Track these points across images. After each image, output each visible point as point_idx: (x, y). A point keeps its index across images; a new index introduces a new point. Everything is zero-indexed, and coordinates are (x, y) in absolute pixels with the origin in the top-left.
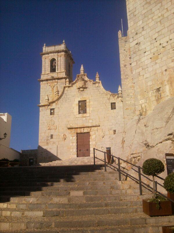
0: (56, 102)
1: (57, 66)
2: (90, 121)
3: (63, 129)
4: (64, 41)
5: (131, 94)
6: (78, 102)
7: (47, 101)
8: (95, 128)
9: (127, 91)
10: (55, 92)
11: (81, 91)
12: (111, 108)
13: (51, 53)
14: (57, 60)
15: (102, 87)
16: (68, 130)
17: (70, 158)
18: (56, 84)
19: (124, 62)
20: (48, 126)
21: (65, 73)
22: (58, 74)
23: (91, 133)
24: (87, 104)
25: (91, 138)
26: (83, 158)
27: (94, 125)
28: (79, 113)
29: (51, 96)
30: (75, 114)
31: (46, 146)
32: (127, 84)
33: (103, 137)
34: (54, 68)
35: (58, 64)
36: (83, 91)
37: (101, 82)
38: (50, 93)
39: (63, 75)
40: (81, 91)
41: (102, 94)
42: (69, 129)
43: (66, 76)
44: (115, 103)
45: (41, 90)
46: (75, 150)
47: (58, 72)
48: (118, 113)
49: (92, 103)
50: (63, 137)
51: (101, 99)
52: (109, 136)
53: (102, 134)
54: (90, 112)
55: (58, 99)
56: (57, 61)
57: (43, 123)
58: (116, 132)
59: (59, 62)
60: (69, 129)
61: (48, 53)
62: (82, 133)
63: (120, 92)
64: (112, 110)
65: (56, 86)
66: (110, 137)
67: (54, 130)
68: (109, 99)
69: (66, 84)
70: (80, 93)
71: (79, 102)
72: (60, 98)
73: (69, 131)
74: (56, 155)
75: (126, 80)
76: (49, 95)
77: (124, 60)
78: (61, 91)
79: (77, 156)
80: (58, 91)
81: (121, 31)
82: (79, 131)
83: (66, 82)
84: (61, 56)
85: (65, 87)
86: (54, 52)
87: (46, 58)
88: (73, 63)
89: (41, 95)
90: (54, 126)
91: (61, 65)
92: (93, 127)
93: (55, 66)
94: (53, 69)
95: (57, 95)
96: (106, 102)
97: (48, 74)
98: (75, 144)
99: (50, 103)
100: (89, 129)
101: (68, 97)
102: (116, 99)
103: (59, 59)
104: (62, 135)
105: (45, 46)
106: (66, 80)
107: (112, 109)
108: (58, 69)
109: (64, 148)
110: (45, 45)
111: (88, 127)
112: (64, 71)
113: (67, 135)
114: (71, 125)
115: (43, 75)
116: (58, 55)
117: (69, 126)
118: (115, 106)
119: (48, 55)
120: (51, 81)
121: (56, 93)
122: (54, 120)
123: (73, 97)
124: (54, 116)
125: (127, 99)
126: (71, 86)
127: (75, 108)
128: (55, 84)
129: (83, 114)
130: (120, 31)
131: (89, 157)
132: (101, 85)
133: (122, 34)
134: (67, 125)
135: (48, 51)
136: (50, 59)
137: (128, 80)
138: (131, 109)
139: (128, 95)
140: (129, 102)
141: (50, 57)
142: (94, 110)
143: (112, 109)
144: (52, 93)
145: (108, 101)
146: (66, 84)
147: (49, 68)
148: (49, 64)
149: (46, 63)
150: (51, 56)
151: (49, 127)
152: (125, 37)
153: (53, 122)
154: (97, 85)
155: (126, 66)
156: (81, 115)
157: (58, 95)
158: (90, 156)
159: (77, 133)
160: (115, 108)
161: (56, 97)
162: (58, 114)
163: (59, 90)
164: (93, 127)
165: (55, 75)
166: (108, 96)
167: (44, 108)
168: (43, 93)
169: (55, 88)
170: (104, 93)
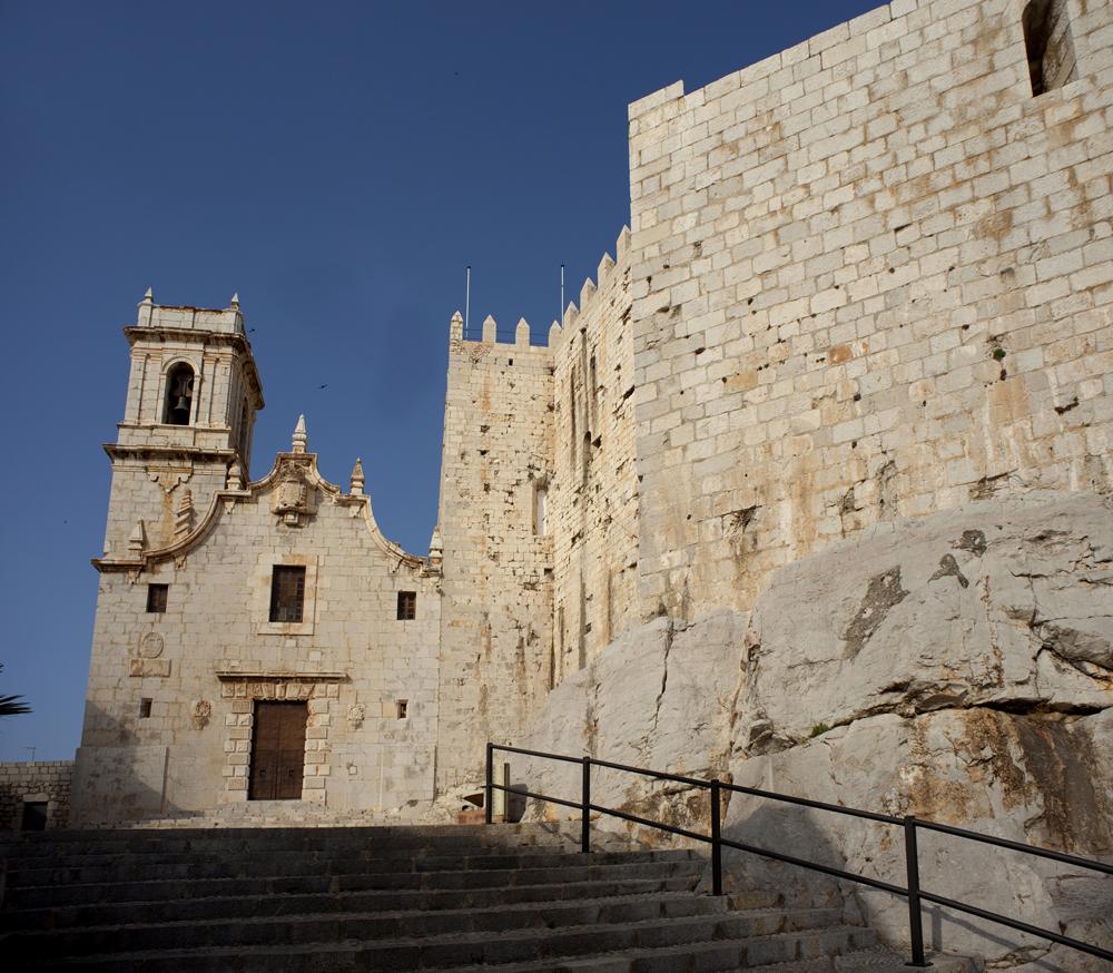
0: (179, 561)
1: (194, 396)
2: (312, 654)
3: (198, 677)
4: (235, 299)
5: (472, 570)
6: (270, 572)
7: (139, 546)
8: (332, 688)
9: (459, 554)
10: (179, 515)
11: (289, 525)
12: (396, 613)
13: (175, 335)
14: (197, 372)
15: (372, 523)
16: (220, 683)
17: (220, 802)
18: (184, 477)
19: (460, 439)
20: (134, 662)
21: (227, 436)
22: (199, 435)
23: (311, 704)
24: (309, 583)
25: (311, 725)
26: (276, 804)
27: (329, 670)
28: (272, 619)
29: (158, 527)
30: (256, 618)
31: (116, 746)
32: (462, 526)
33: (358, 726)
34: (180, 405)
35: (200, 392)
36: (295, 526)
37: (369, 501)
38: (153, 512)
39: (221, 444)
40: (289, 525)
41: (369, 549)
42: (225, 679)
43: (232, 452)
44: (412, 596)
45: (114, 494)
46: (242, 771)
47: (199, 426)
48: (420, 635)
49: (325, 582)
50: (194, 712)
51: (365, 571)
52: (381, 721)
53: (356, 714)
54: (317, 621)
55: (188, 548)
56: (197, 380)
57: (112, 643)
58: (405, 709)
59: (206, 387)
60: (225, 679)
61: (161, 336)
62: (276, 702)
63: (437, 554)
64: (401, 622)
65: (183, 486)
66: (383, 727)
67: (160, 679)
68: (393, 575)
69: (226, 487)
70: (286, 532)
71: (277, 569)
72: (200, 544)
73: (224, 689)
74: (158, 787)
75: (460, 512)
76: (150, 522)
77: (462, 433)
78: (204, 509)
79: (250, 797)
80: (191, 510)
81: (464, 316)
82: (265, 692)
83: (228, 477)
84: (218, 360)
85: (222, 499)
86: (187, 336)
87: (148, 356)
88: (260, 405)
89: (111, 516)
90: (160, 663)
91: (215, 398)
92: (324, 679)
93: (188, 401)
94: (177, 413)
95: (183, 527)
96: (380, 586)
97: (152, 428)
98: (244, 746)
99: (148, 558)
100: (306, 688)
101: (232, 541)
102: (419, 580)
103: (209, 369)
104: (194, 703)
105: (148, 301)
106: (229, 467)
107: (398, 619)
108: (197, 412)
109: (198, 761)
110: (149, 294)
111: (304, 680)
112: (222, 426)
113: (212, 703)
114: (234, 663)
115: (131, 430)
116: (205, 353)
117: (224, 669)
118: (412, 605)
119: (160, 345)
120: (165, 463)
121: (183, 517)
122: (163, 634)
123: (254, 544)
124: (165, 616)
125: (459, 585)
126: (247, 497)
127: (257, 595)
128: (179, 475)
129: (287, 624)
130: (458, 313)
131: (298, 801)
132: (368, 511)
133: (464, 330)
134: (216, 662)
135: (163, 325)
136: (171, 363)
137: (470, 513)
138: (466, 627)
139: (462, 571)
140: (464, 601)
141: (171, 356)
142: (332, 613)
143: (400, 617)
144: (162, 517)
145: (388, 581)
146: (226, 487)
147: (161, 403)
148: (163, 385)
149: (148, 376)
150: (175, 352)
151: (135, 665)
152: (476, 343)
153: (156, 644)
154: (354, 510)
155: (467, 458)
156: (280, 625)
157: (190, 530)
158: (300, 798)
159: (258, 703)
160: (411, 617)
161: (180, 536)
162: (182, 613)
163: (196, 508)
164: (324, 679)
165: (181, 438)
166: (392, 561)
167: (118, 577)
168: (122, 511)
169: (178, 496)
170: (377, 548)
